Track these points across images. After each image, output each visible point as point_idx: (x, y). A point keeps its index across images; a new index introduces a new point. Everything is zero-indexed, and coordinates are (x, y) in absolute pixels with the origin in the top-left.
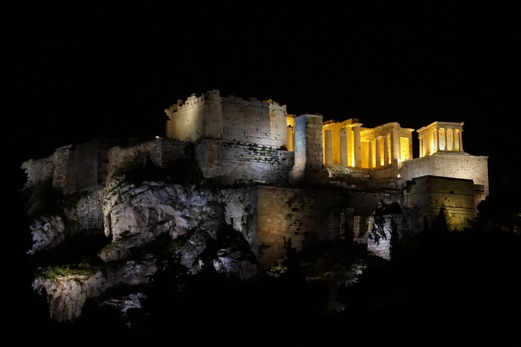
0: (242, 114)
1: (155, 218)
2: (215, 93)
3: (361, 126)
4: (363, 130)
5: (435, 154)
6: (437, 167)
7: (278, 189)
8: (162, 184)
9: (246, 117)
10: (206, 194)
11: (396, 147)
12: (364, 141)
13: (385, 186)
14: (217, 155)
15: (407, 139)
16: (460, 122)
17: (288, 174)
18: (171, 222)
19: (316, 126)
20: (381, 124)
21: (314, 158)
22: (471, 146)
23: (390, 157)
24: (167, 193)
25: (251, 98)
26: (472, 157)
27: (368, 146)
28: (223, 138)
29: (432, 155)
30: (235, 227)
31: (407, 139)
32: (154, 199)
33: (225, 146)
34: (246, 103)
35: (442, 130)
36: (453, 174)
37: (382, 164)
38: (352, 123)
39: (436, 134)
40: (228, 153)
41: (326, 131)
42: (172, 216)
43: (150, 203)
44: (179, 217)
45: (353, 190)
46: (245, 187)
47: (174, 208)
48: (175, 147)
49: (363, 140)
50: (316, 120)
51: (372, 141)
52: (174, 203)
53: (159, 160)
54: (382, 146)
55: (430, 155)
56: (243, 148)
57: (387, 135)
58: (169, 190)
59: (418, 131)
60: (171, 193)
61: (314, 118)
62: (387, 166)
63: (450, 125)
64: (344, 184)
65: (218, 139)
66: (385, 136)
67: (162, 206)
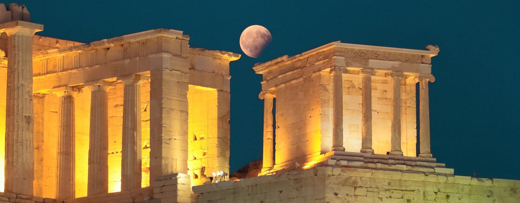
4: (43, 49)
5: (322, 164)
11: (173, 124)
12: (43, 91)
15: (213, 92)
20: (114, 32)
26: (464, 180)
31: (213, 92)
49: (40, 85)
51: (75, 95)
55: (308, 166)
57: (138, 78)
63: (387, 57)
66: (130, 81)
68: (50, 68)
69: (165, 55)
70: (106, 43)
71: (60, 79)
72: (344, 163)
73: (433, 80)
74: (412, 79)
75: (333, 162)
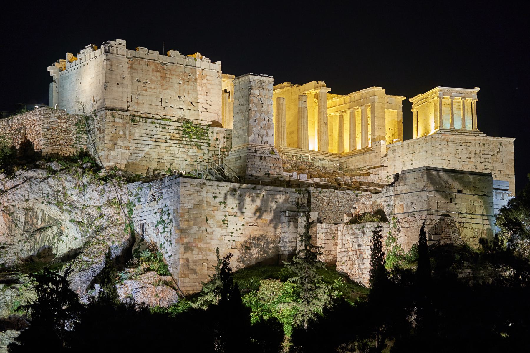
1: (33, 223)
2: (120, 44)
3: (329, 92)
4: (332, 98)
5: (435, 133)
7: (207, 183)
8: (45, 174)
9: (163, 78)
10: (106, 189)
12: (332, 114)
13: (362, 179)
14: (121, 133)
16: (473, 88)
17: (222, 161)
18: (55, 228)
19: (263, 93)
21: (260, 138)
22: (490, 121)
23: (370, 137)
24: (51, 187)
25: (171, 52)
26: (491, 138)
27: (337, 120)
29: (432, 136)
30: (146, 237)
32: (32, 196)
33: (133, 121)
35: (447, 100)
36: (462, 163)
37: (359, 147)
38: (316, 88)
39: (438, 105)
40: (137, 131)
41: (278, 99)
42: (56, 220)
43: (27, 200)
44: (67, 223)
45: (318, 185)
46: (161, 180)
47: (61, 209)
48: (63, 121)
49: (331, 112)
50: (263, 84)
51: (344, 114)
52: (59, 200)
54: (358, 121)
55: (429, 134)
56: (160, 124)
58: (52, 181)
59: (411, 100)
60: (56, 188)
61: (261, 81)
62: (367, 150)
64: (304, 177)
65: (122, 110)
66: (363, 107)
67: (43, 207)
68: (334, 105)
69: (376, 97)
70: (354, 94)
71: (338, 108)
72: (443, 132)
73: (478, 100)
74: (469, 100)
75: (439, 132)
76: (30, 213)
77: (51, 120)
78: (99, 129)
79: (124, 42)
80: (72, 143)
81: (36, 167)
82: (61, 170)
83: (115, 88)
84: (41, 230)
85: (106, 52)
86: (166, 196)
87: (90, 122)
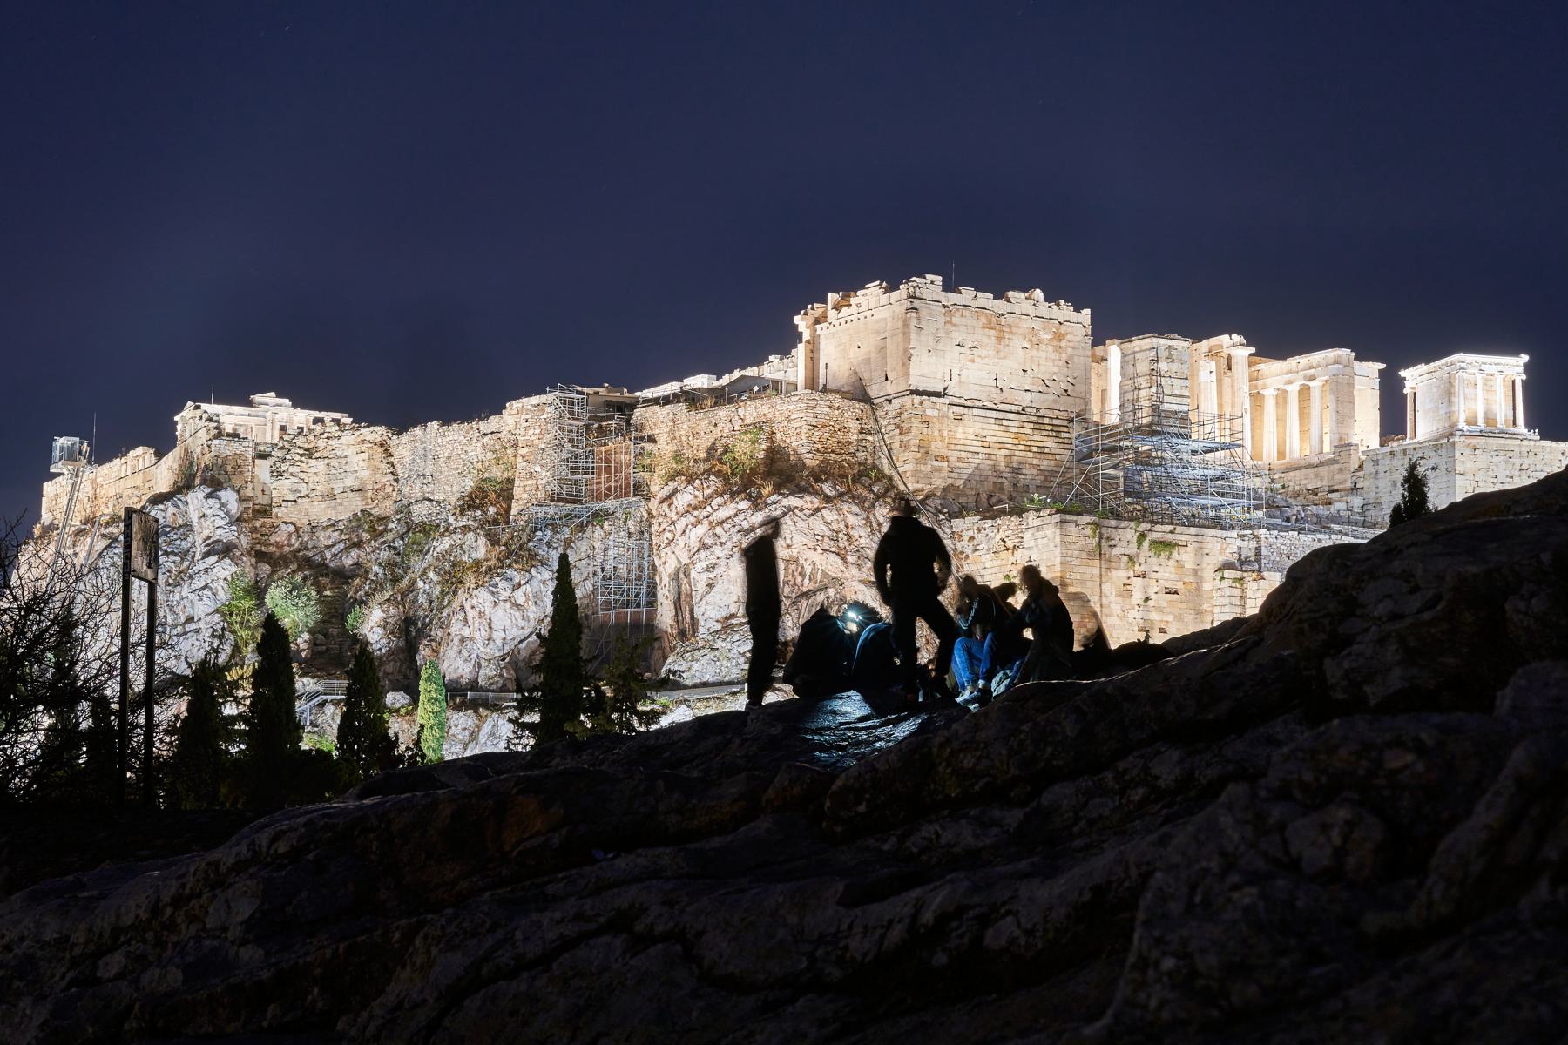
0: (992, 332)
6: (1459, 468)
8: (817, 502)
9: (1000, 339)
18: (831, 592)
26: (1548, 443)
28: (949, 392)
34: (1000, 305)
53: (800, 443)
59: (1403, 373)
60: (834, 526)
65: (937, 395)
67: (816, 557)
76: (793, 567)
77: (818, 410)
78: (897, 426)
79: (938, 279)
80: (852, 449)
81: (800, 491)
82: (841, 495)
83: (925, 356)
84: (806, 595)
85: (909, 297)
86: (1032, 543)
87: (880, 413)
